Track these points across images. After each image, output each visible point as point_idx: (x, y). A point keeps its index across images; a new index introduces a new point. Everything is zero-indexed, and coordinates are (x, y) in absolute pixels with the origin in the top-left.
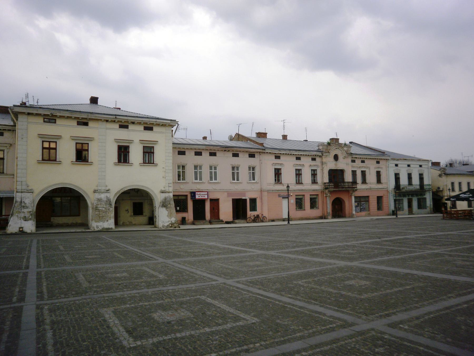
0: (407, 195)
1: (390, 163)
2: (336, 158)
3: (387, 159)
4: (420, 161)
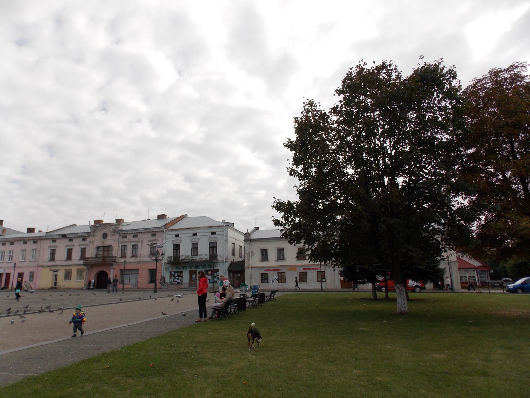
0: (189, 266)
1: (168, 235)
2: (105, 236)
3: (162, 231)
4: (212, 228)
